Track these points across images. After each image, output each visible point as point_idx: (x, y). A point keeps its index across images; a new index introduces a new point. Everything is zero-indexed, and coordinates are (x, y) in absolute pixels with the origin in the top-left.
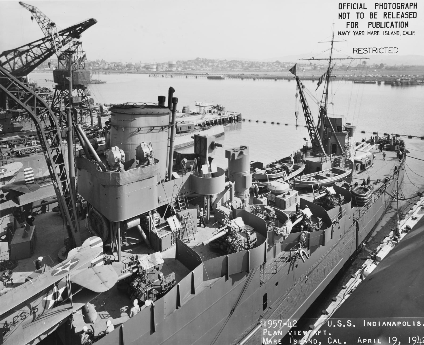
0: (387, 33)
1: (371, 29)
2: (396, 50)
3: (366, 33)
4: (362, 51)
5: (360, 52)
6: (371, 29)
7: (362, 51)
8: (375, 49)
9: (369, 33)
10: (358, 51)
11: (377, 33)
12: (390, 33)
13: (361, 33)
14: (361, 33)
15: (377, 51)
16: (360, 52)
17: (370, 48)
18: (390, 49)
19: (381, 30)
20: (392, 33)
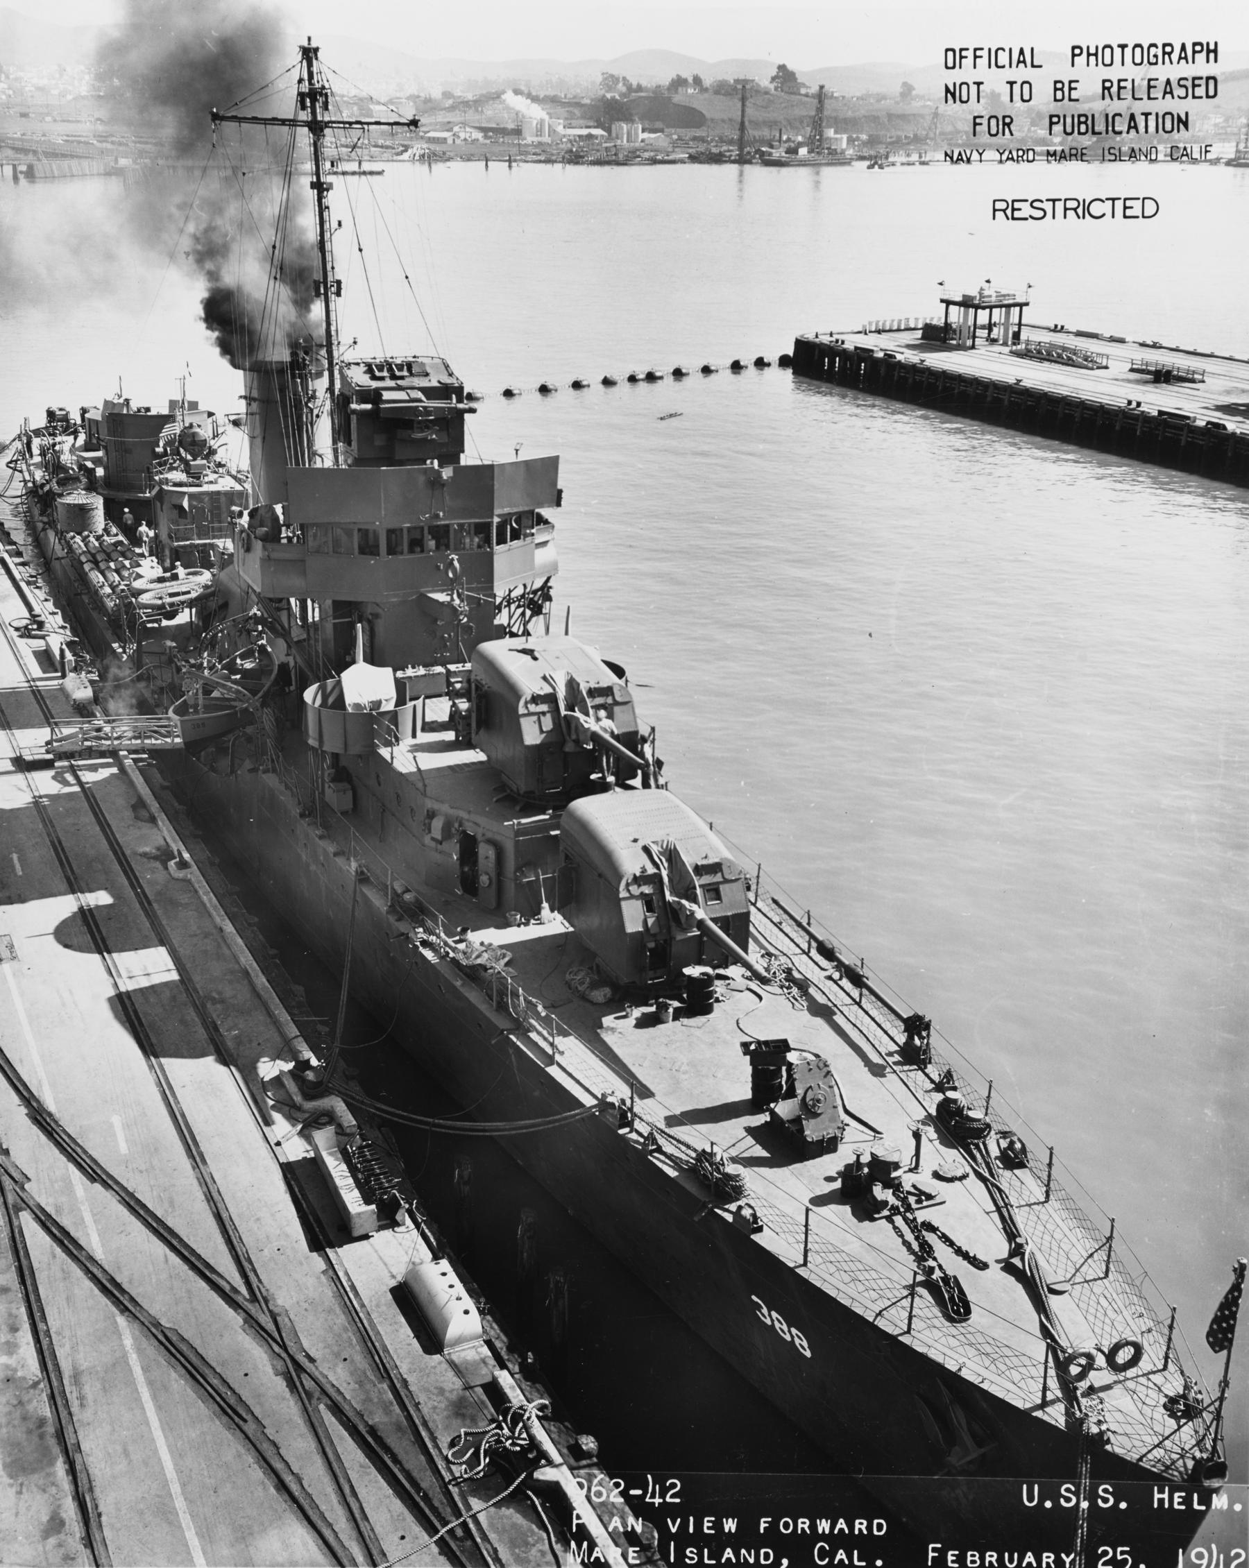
4: (1026, 210)
5: (1017, 214)
7: (1026, 210)
8: (1074, 204)
10: (1009, 212)
15: (1080, 211)
16: (1017, 214)
17: (1054, 201)
18: (1128, 203)
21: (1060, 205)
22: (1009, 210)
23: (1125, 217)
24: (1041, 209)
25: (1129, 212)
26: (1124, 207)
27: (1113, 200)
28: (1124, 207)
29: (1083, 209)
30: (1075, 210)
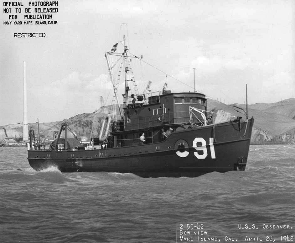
0: (37, 23)
1: (27, 20)
2: (44, 35)
3: (23, 23)
4: (21, 35)
6: (27, 20)
7: (21, 35)
8: (30, 34)
11: (31, 23)
12: (39, 23)
13: (20, 23)
14: (20, 23)
15: (31, 36)
17: (26, 34)
18: (40, 34)
19: (33, 21)
20: (41, 23)
23: (39, 37)
24: (24, 35)
25: (40, 36)
26: (39, 35)
27: (37, 33)
28: (39, 35)
29: (31, 35)
30: (30, 35)
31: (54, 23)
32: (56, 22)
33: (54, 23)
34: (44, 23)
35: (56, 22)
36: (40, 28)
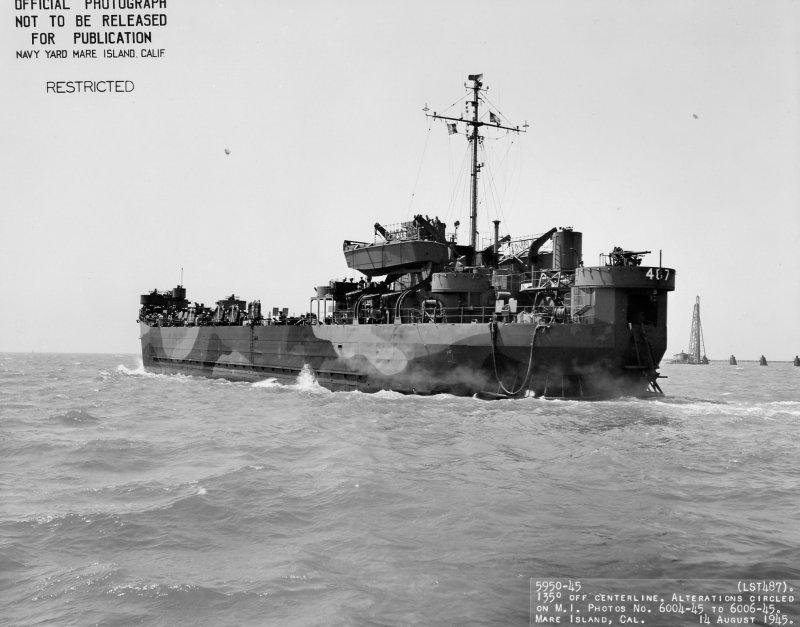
0: (110, 54)
4: (64, 87)
7: (64, 87)
8: (88, 84)
9: (75, 54)
10: (55, 88)
11: (92, 53)
12: (117, 54)
13: (61, 54)
14: (61, 54)
21: (82, 85)
22: (55, 87)
24: (72, 86)
25: (119, 89)
26: (116, 85)
28: (116, 85)
29: (94, 87)
31: (156, 54)
32: (161, 52)
33: (156, 54)
34: (130, 53)
35: (161, 52)
36: (119, 69)
